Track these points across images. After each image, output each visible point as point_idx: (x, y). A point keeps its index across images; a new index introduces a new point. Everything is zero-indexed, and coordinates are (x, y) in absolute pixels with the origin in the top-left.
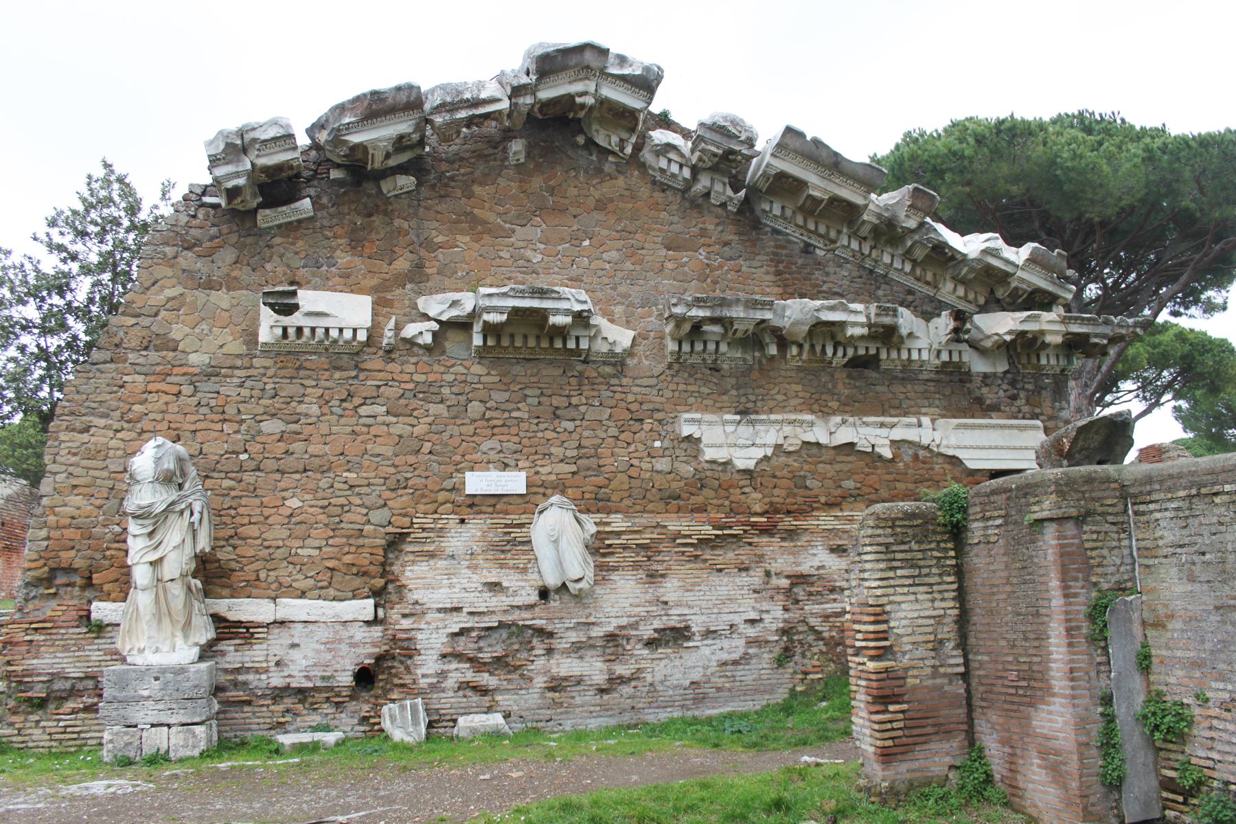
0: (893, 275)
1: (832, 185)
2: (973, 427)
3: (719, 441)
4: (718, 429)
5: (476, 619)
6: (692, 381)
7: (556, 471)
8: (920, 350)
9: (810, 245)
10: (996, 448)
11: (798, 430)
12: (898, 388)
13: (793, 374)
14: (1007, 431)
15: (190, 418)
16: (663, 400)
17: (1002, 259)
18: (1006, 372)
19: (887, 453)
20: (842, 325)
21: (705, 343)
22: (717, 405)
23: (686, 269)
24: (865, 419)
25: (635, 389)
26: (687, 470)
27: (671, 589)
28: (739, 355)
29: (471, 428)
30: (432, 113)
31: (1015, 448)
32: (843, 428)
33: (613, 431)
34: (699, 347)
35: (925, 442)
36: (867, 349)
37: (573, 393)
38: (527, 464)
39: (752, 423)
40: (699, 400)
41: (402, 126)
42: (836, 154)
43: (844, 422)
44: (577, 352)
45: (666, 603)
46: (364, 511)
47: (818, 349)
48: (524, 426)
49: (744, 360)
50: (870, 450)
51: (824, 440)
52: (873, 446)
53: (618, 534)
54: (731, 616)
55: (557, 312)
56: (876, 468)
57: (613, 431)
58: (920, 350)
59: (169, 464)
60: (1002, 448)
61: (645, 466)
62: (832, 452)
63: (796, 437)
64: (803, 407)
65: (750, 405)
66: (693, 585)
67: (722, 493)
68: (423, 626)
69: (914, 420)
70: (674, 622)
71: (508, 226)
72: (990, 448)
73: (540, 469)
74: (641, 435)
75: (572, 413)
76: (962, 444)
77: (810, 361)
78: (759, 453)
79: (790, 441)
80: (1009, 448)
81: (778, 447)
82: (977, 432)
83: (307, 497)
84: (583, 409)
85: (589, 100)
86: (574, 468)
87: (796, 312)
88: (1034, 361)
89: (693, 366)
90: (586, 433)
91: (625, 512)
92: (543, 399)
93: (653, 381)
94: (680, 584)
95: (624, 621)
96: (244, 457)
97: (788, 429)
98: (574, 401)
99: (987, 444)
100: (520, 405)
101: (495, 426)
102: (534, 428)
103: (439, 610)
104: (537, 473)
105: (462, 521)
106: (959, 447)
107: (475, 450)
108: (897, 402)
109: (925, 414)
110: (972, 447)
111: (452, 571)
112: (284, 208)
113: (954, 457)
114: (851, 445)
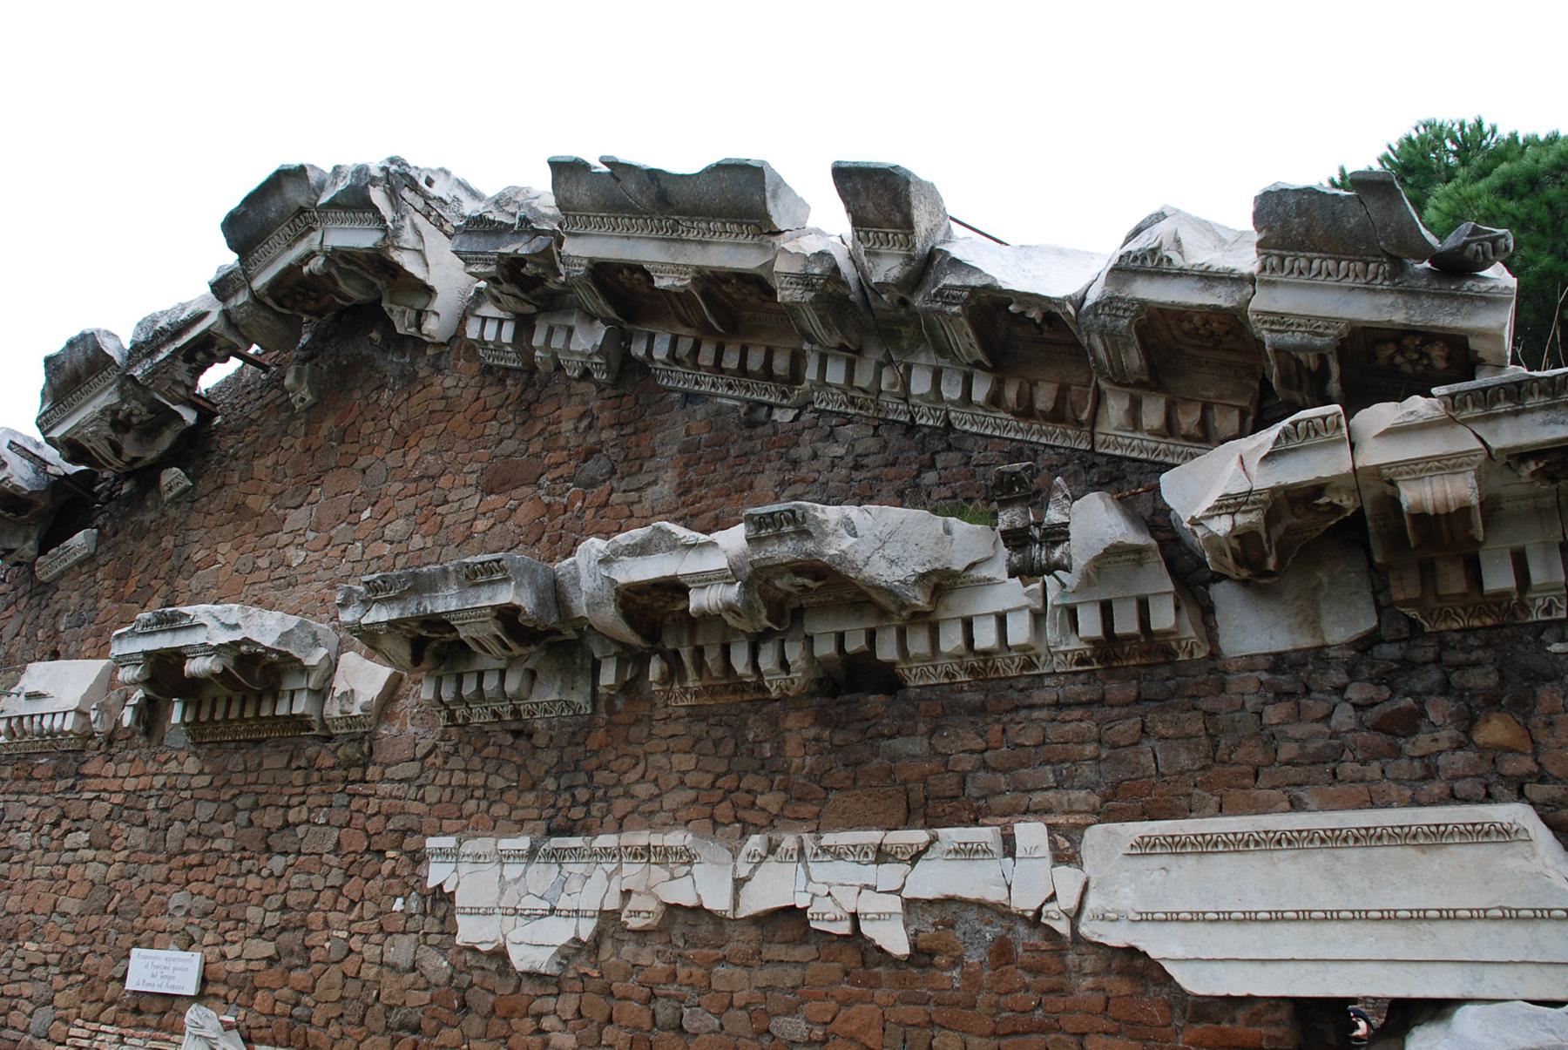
0: (964, 422)
1: (692, 248)
2: (1207, 846)
4: (490, 872)
6: (477, 760)
8: (1001, 619)
9: (761, 404)
10: (1303, 917)
11: (659, 873)
12: (961, 742)
13: (679, 728)
14: (1354, 855)
16: (422, 808)
17: (1182, 274)
18: (1365, 644)
19: (894, 938)
20: (675, 588)
21: (481, 675)
22: (517, 815)
23: (510, 524)
24: (829, 839)
25: (385, 788)
26: (437, 965)
28: (555, 697)
29: (164, 868)
30: (129, 367)
31: (1388, 917)
32: (771, 866)
33: (335, 878)
34: (469, 688)
35: (1025, 900)
36: (841, 638)
37: (295, 801)
38: (209, 938)
39: (557, 856)
40: (484, 804)
41: (106, 398)
42: (654, 175)
43: (772, 849)
44: (301, 722)
47: (712, 657)
48: (223, 863)
49: (569, 704)
50: (844, 928)
51: (717, 899)
52: (855, 917)
56: (876, 983)
57: (335, 878)
58: (1001, 619)
60: (1332, 917)
61: (371, 952)
62: (753, 932)
63: (649, 891)
64: (693, 812)
65: (577, 813)
69: (986, 834)
72: (1277, 917)
75: (287, 841)
76: (1159, 909)
77: (712, 691)
78: (560, 932)
79: (635, 903)
80: (1361, 917)
81: (609, 918)
82: (1223, 865)
84: (301, 830)
85: (317, 264)
86: (268, 949)
87: (599, 567)
88: (1453, 582)
89: (482, 732)
92: (255, 815)
93: (412, 769)
97: (633, 873)
98: (293, 816)
99: (1261, 904)
101: (191, 867)
102: (234, 868)
104: (224, 956)
106: (1146, 918)
107: (164, 909)
108: (951, 780)
109: (1029, 812)
110: (1198, 918)
112: (54, 550)
113: (1132, 952)
114: (793, 914)
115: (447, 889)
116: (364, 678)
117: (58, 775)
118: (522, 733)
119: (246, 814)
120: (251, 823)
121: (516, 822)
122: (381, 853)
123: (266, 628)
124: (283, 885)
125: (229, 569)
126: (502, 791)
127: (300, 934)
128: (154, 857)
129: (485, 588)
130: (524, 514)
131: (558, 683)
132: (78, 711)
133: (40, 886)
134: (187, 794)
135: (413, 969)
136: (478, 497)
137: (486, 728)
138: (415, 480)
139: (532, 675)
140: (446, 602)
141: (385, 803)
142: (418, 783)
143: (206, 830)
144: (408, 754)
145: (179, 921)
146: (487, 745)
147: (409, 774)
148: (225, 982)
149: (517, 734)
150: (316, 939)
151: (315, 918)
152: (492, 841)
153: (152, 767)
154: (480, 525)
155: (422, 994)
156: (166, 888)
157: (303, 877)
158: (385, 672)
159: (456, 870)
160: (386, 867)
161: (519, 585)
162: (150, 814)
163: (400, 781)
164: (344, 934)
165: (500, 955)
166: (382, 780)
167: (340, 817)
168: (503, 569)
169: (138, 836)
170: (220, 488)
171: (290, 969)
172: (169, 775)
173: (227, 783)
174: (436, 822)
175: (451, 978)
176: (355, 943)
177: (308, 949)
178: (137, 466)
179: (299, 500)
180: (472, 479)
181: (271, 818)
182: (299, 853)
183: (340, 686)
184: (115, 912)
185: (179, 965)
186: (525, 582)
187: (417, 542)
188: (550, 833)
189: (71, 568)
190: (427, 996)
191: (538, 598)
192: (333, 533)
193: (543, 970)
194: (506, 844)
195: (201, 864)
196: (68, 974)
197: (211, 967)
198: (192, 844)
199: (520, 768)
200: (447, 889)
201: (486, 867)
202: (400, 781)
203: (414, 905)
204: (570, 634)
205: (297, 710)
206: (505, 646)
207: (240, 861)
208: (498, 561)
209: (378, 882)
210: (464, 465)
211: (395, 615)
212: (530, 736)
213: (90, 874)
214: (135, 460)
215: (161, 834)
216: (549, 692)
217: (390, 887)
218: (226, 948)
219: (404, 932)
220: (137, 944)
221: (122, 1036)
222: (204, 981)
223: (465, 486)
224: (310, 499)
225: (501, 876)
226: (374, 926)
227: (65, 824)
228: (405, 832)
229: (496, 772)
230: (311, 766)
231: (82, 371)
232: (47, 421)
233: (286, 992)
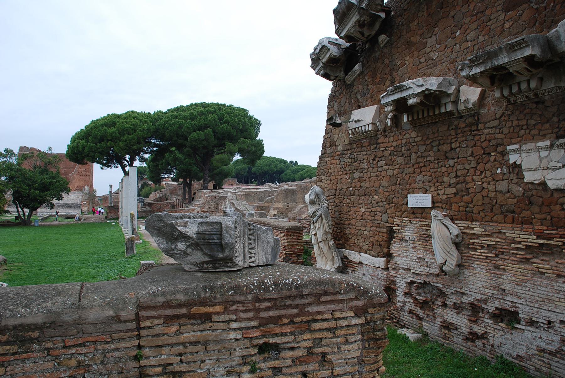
3: (533, 166)
4: (535, 156)
5: (416, 277)
6: (522, 116)
7: (446, 193)
15: (340, 173)
16: (503, 136)
21: (519, 84)
25: (486, 131)
26: (518, 190)
27: (507, 281)
30: (360, 4)
33: (473, 164)
34: (515, 89)
37: (453, 140)
38: (432, 189)
40: (527, 131)
44: (450, 113)
45: (504, 290)
46: (381, 214)
48: (432, 165)
49: (559, 88)
53: (478, 236)
54: (549, 314)
55: (410, 97)
59: (313, 197)
61: (491, 188)
66: (521, 281)
67: (545, 209)
68: (398, 276)
70: (507, 306)
71: (425, 40)
73: (439, 192)
74: (489, 165)
75: (453, 154)
83: (366, 207)
84: (458, 150)
86: (454, 190)
89: (522, 104)
90: (459, 167)
91: (481, 220)
92: (440, 147)
93: (496, 123)
94: (513, 278)
95: (479, 297)
96: (351, 189)
98: (453, 146)
100: (430, 153)
101: (421, 167)
102: (436, 166)
103: (404, 269)
104: (438, 194)
105: (410, 222)
111: (407, 249)
115: (518, 163)
116: (471, 94)
117: (371, 144)
118: (539, 102)
119: (437, 148)
120: (439, 150)
121: (542, 136)
122: (489, 154)
123: (433, 83)
124: (455, 169)
125: (411, 65)
126: (534, 125)
127: (464, 184)
128: (408, 166)
129: (519, 51)
130: (525, 16)
131: (554, 80)
132: (372, 123)
133: (374, 179)
134: (415, 144)
135: (508, 192)
136: (504, 15)
137: (524, 103)
138: (475, 15)
139: (541, 80)
140: (503, 59)
141: (487, 136)
142: (499, 127)
143: (424, 154)
144: (493, 118)
145: (421, 184)
146: (525, 109)
147: (495, 125)
148: (441, 202)
149: (537, 103)
150: (470, 185)
151: (468, 179)
152: (533, 144)
153: (400, 137)
154: (507, 25)
155: (513, 200)
156: (414, 175)
157: (462, 166)
158: (479, 90)
159: (520, 156)
160: (492, 158)
161: (533, 47)
162: (404, 152)
163: (492, 128)
164: (481, 183)
165: (543, 184)
166: (485, 128)
167: (472, 143)
168: (526, 42)
169: (401, 160)
170: (400, 37)
171: (462, 196)
172: (407, 139)
173: (428, 138)
174: (509, 140)
175: (524, 194)
176: (485, 185)
177: (468, 189)
178: (369, 38)
179: (430, 34)
180: (500, 8)
181: (446, 148)
182: (458, 158)
183: (463, 98)
184: (399, 184)
185: (424, 198)
186: (535, 44)
187: (481, 38)
188: (558, 138)
189: (356, 77)
190: (515, 201)
191: (542, 49)
192: (447, 43)
193: (562, 188)
194: (539, 144)
195: (424, 166)
196: (389, 204)
197: (435, 198)
198: (420, 160)
199: (540, 116)
200: (518, 163)
201: (533, 153)
202: (492, 128)
203: (505, 170)
204: (557, 60)
205: (449, 109)
206: (529, 71)
207: (438, 163)
208: (523, 39)
209: (490, 164)
210: (495, 3)
211: (483, 69)
212: (543, 103)
213: (388, 173)
214: (369, 36)
215: (409, 158)
216: (550, 85)
217: (495, 165)
218: (439, 192)
219: (503, 180)
220: (409, 193)
221: (410, 221)
222: (433, 202)
223: (497, 11)
224: (435, 33)
225: (539, 156)
226: (491, 179)
227: (377, 159)
228: (497, 145)
229: (531, 119)
230: (457, 127)
231: (345, 11)
232: (339, 31)
233: (462, 203)
